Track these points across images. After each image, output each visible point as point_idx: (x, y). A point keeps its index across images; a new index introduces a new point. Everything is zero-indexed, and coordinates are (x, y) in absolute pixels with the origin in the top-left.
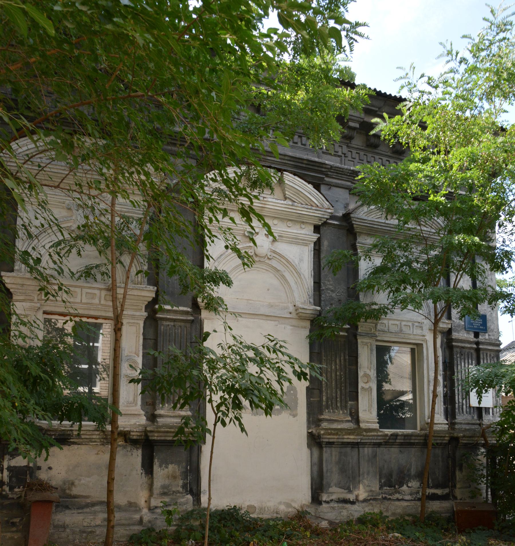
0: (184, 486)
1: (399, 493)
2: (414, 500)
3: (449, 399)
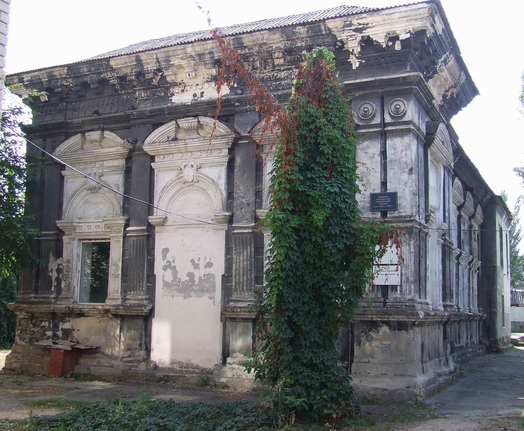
0: (140, 345)
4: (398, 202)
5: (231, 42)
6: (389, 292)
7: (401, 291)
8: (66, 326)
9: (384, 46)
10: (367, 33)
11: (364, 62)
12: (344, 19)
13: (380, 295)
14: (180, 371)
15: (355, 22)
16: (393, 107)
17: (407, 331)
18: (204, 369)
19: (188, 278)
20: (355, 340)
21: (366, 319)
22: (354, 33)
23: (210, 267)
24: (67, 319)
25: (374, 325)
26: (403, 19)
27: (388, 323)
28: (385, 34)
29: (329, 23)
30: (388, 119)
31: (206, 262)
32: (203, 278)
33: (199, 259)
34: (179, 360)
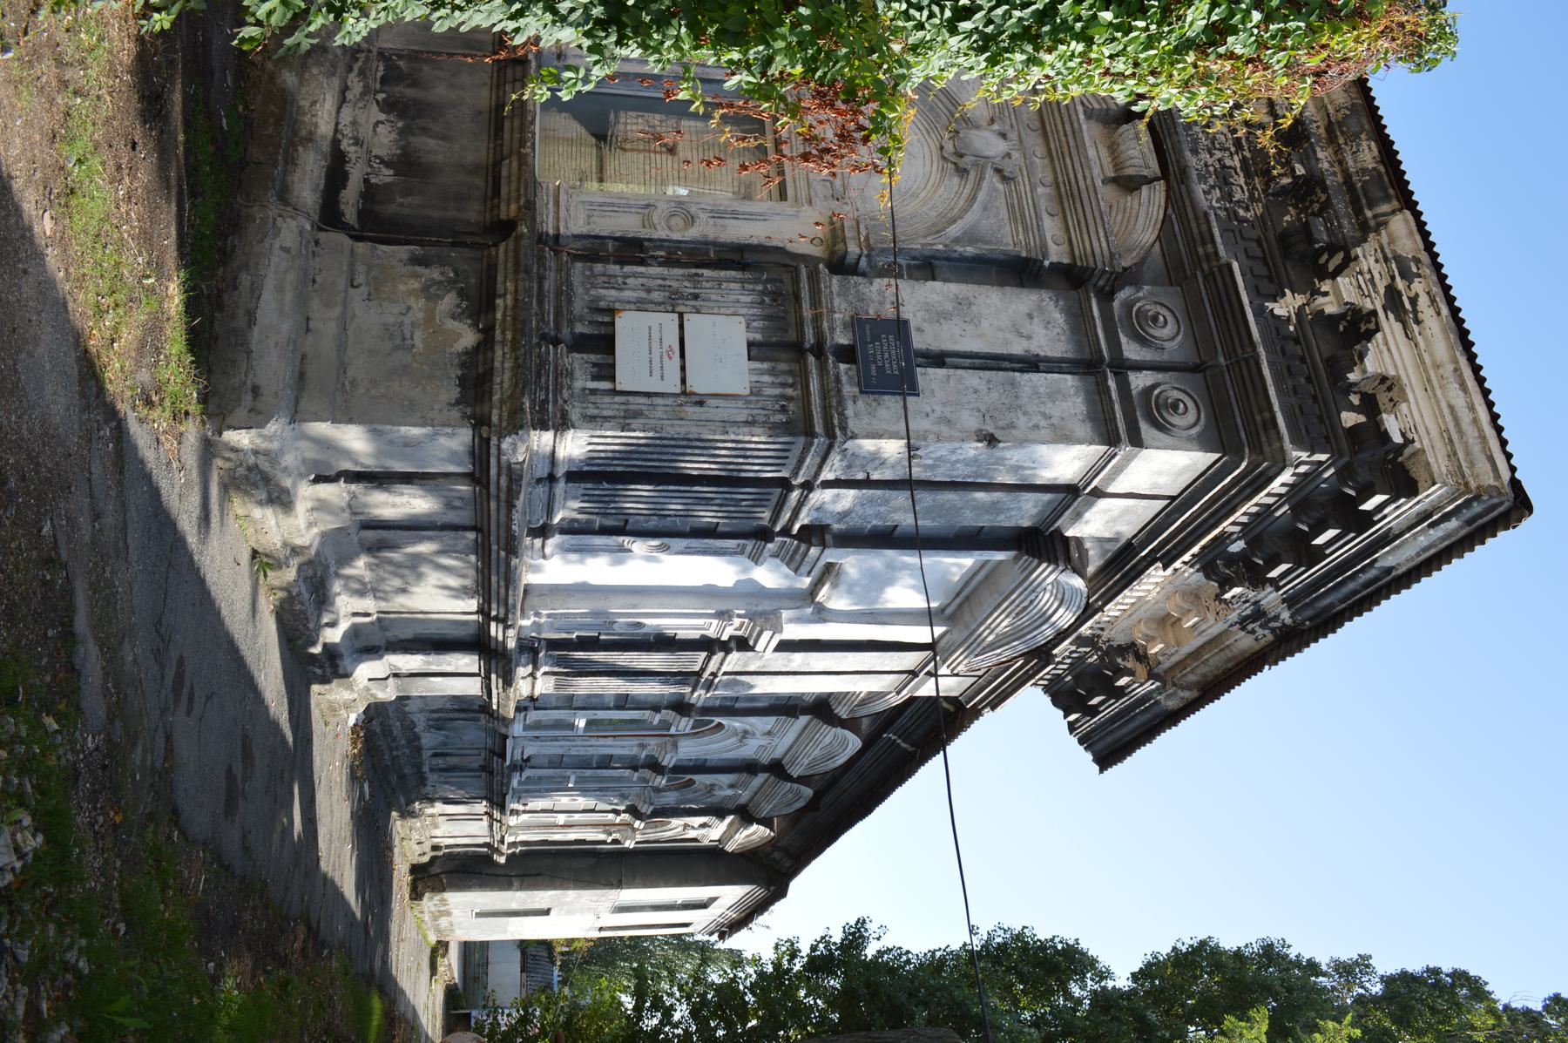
1: (363, 94)
2: (336, 131)
3: (631, 250)
4: (886, 397)
6: (593, 358)
7: (593, 392)
9: (1353, 377)
10: (1390, 326)
11: (1292, 328)
13: (580, 328)
15: (1418, 287)
16: (1176, 394)
17: (458, 402)
20: (433, 251)
21: (500, 278)
22: (1382, 291)
25: (479, 306)
26: (1449, 418)
27: (487, 342)
28: (1392, 372)
29: (1406, 220)
30: (1139, 381)
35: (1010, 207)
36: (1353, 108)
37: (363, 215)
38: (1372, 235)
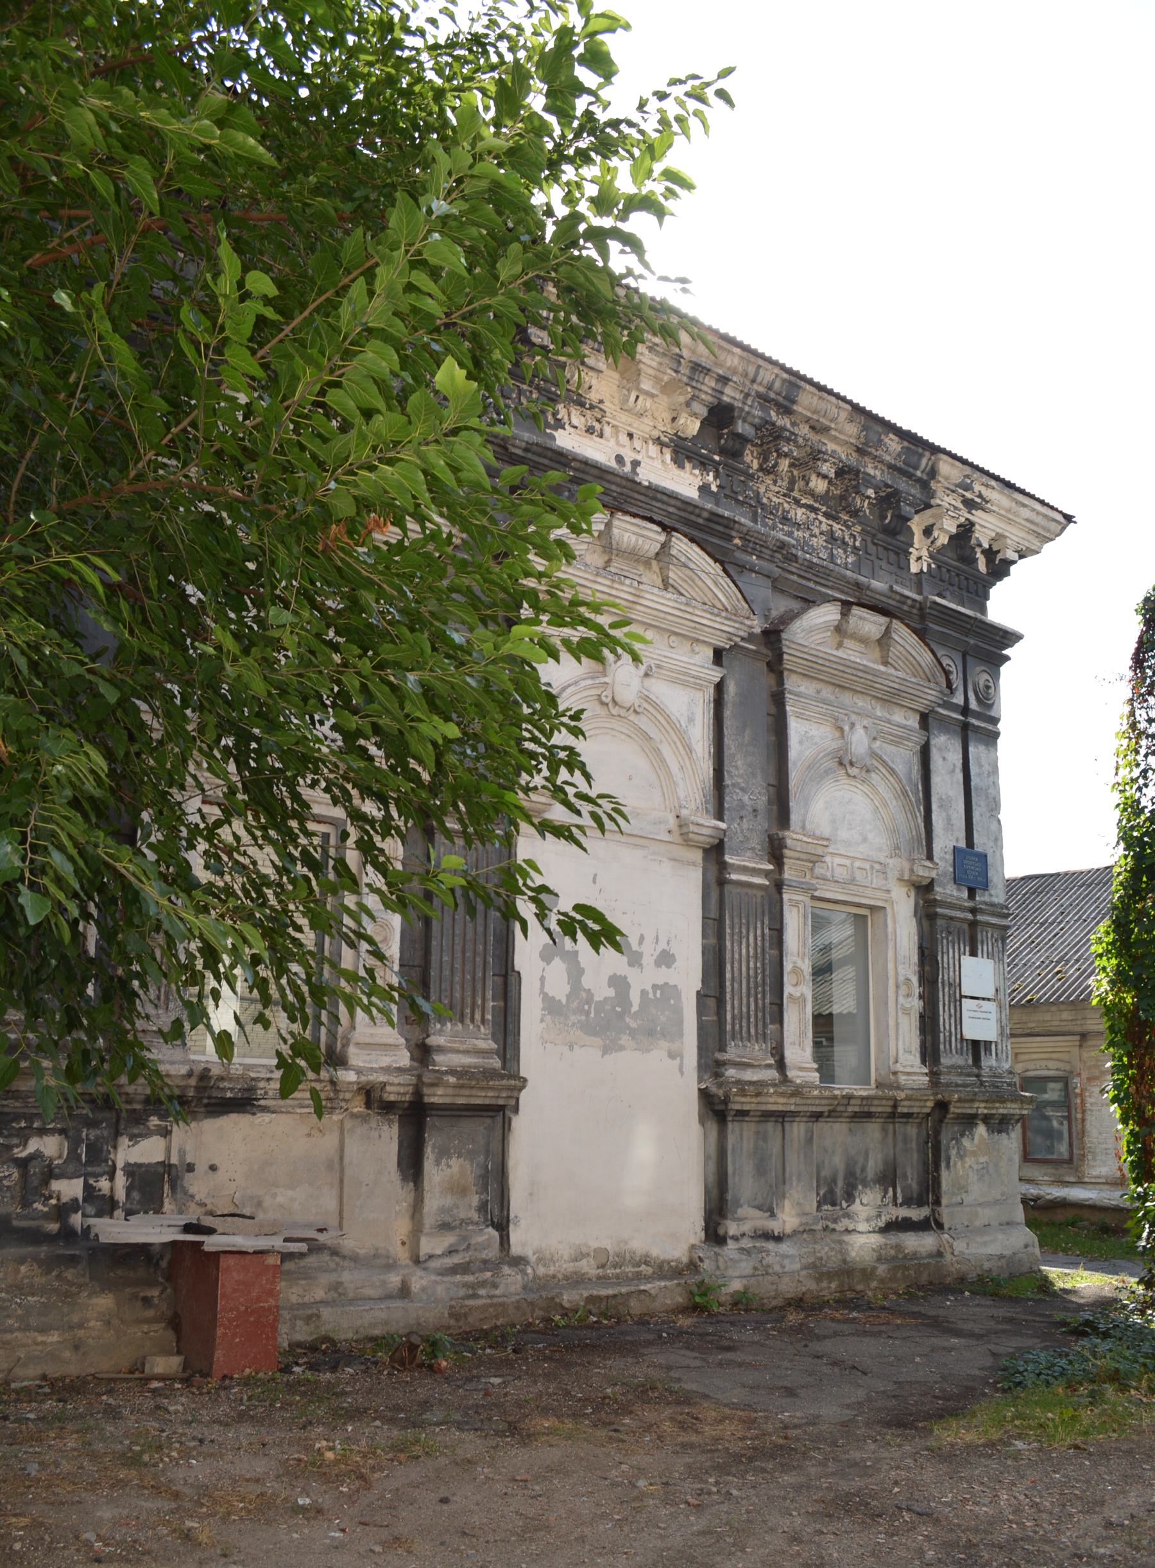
3: (928, 1024)
5: (777, 385)
8: (147, 1151)
12: (968, 470)
13: (970, 1062)
14: (599, 1278)
15: (977, 487)
18: (663, 1262)
19: (611, 993)
22: (961, 506)
23: (669, 967)
24: (154, 1121)
31: (659, 949)
32: (651, 996)
33: (642, 938)
34: (594, 1244)
35: (892, 743)
36: (865, 428)
37: (921, 1203)
38: (933, 484)
